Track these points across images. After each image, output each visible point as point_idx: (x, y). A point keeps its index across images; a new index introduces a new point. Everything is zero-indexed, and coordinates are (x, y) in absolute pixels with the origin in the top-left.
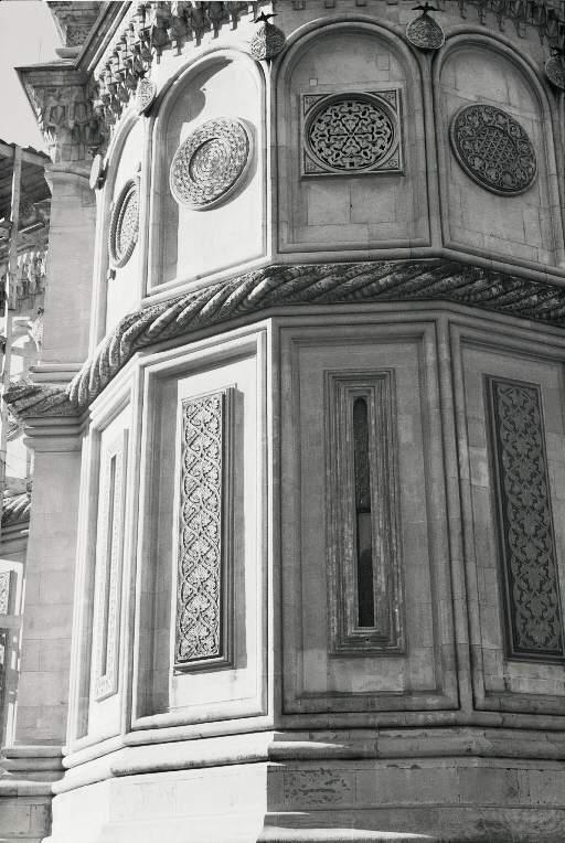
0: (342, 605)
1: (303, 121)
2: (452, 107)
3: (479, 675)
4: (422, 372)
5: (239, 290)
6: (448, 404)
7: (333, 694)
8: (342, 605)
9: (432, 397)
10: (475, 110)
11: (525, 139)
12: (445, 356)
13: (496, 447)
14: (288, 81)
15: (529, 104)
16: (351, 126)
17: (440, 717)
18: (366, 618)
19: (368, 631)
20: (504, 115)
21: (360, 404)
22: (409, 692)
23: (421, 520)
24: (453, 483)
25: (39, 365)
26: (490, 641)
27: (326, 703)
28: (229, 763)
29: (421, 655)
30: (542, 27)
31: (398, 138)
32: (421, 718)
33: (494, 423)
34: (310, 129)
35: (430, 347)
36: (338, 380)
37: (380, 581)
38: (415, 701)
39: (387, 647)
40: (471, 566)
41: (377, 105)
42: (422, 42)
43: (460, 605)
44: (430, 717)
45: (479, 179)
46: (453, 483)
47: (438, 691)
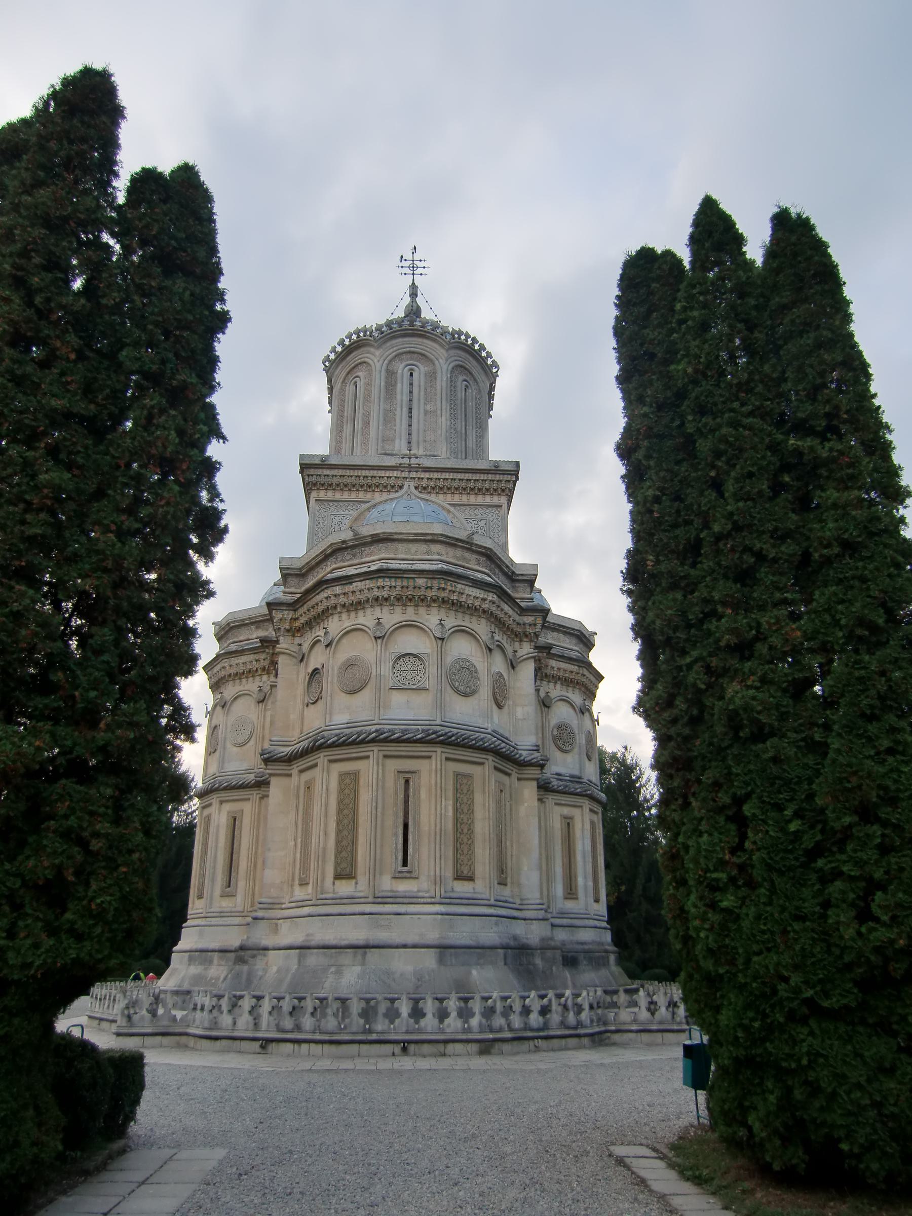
0: (396, 859)
1: (391, 663)
2: (449, 660)
3: (442, 886)
4: (430, 771)
5: (364, 736)
6: (439, 785)
7: (392, 891)
8: (396, 859)
9: (433, 782)
10: (457, 661)
11: (476, 672)
12: (439, 767)
13: (456, 800)
14: (386, 645)
15: (479, 654)
16: (409, 667)
17: (429, 900)
18: (405, 863)
19: (405, 869)
20: (468, 661)
21: (407, 782)
22: (418, 891)
23: (427, 828)
24: (438, 815)
25: (273, 739)
26: (449, 873)
27: (389, 894)
28: (354, 914)
29: (423, 878)
30: (487, 619)
31: (427, 674)
32: (422, 900)
33: (456, 790)
34: (394, 667)
35: (434, 762)
37: (410, 851)
38: (421, 894)
39: (411, 876)
40: (443, 847)
41: (420, 659)
42: (439, 635)
43: (438, 861)
44: (425, 900)
45: (457, 691)
46: (438, 815)
47: (427, 892)
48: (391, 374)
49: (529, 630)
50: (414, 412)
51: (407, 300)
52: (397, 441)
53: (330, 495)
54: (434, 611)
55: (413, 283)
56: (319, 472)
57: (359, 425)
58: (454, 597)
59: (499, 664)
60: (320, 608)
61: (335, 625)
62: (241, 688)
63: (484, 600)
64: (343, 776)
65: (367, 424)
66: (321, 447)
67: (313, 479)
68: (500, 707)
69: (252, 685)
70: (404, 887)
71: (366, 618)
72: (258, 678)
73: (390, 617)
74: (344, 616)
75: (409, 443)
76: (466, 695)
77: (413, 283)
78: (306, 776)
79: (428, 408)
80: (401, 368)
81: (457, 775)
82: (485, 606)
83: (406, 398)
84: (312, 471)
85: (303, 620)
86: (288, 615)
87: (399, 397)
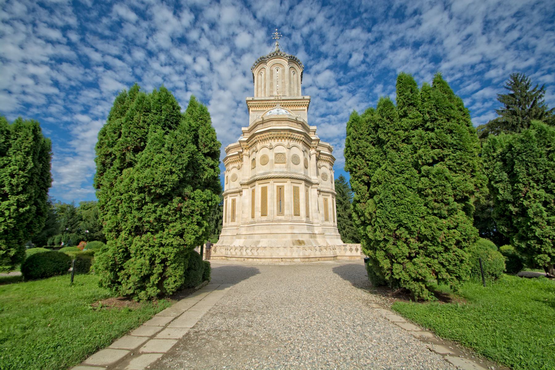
36: (278, 186)
53: (255, 109)
54: (287, 140)
57: (263, 88)
58: (292, 136)
60: (254, 141)
61: (259, 146)
64: (262, 188)
65: (265, 87)
69: (236, 165)
70: (280, 217)
71: (267, 144)
73: (274, 143)
78: (253, 188)
80: (274, 69)
81: (294, 187)
82: (301, 139)
85: (250, 145)
86: (246, 144)
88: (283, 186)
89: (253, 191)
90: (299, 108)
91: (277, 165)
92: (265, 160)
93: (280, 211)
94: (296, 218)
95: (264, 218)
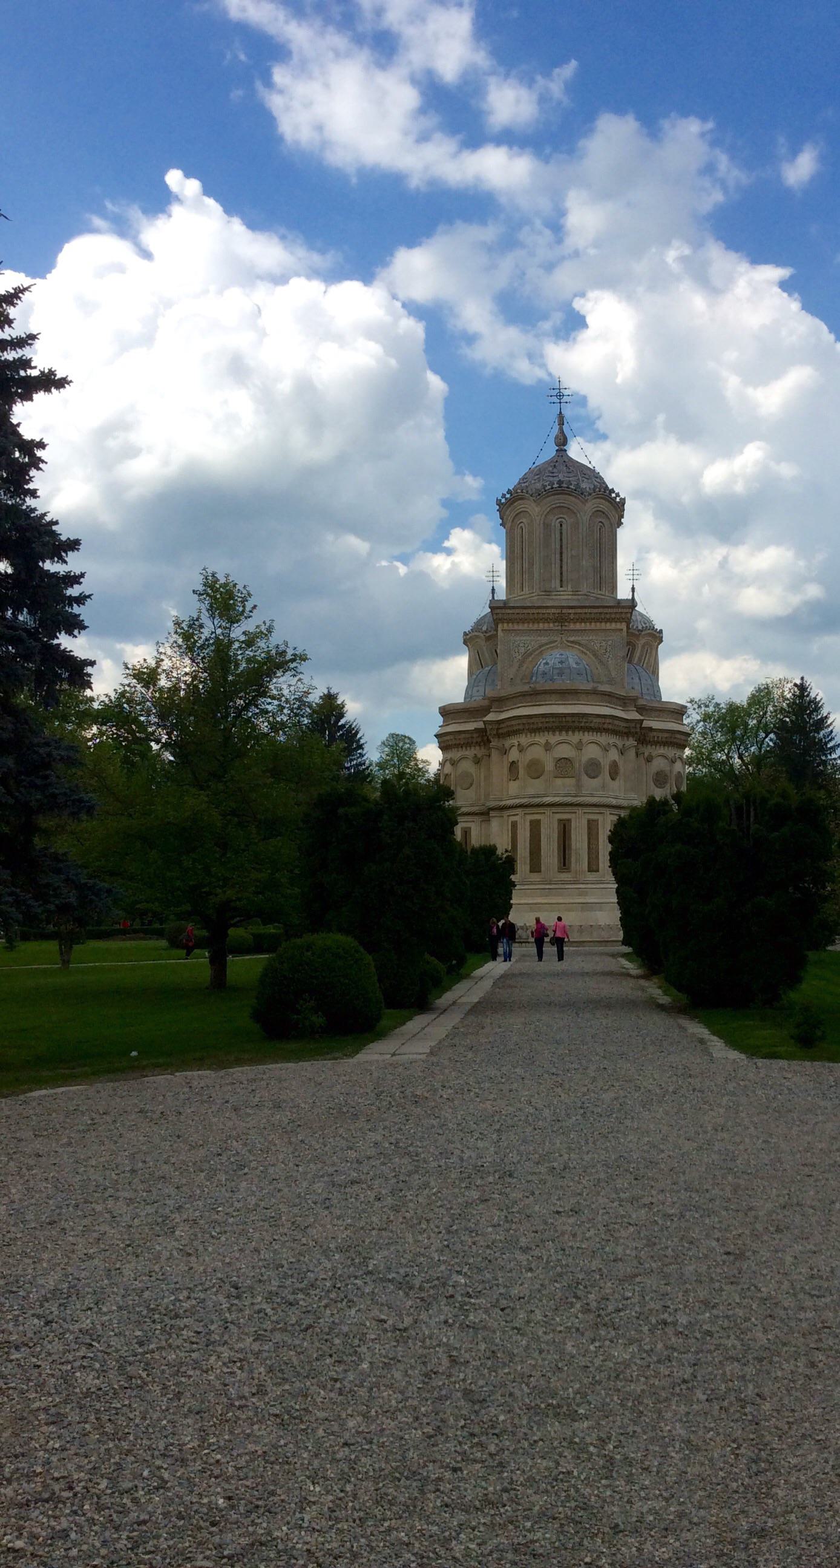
2: (584, 759)
36: (560, 820)
48: (547, 526)
49: (633, 730)
50: (564, 556)
51: (556, 428)
52: (553, 581)
54: (577, 733)
55: (561, 413)
56: (503, 611)
57: (526, 565)
59: (614, 755)
62: (462, 753)
63: (604, 723)
64: (531, 822)
65: (531, 564)
66: (501, 595)
67: (500, 616)
68: (613, 779)
69: (470, 752)
70: (565, 876)
71: (541, 739)
72: (473, 748)
73: (553, 738)
74: (529, 736)
75: (561, 581)
76: (594, 778)
77: (561, 413)
79: (573, 553)
81: (589, 821)
83: (558, 547)
84: (498, 611)
87: (553, 544)
88: (569, 820)
89: (514, 825)
90: (608, 626)
91: (559, 781)
92: (535, 770)
93: (564, 865)
94: (591, 877)
95: (535, 877)
